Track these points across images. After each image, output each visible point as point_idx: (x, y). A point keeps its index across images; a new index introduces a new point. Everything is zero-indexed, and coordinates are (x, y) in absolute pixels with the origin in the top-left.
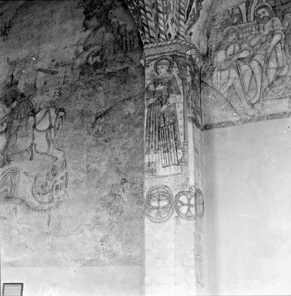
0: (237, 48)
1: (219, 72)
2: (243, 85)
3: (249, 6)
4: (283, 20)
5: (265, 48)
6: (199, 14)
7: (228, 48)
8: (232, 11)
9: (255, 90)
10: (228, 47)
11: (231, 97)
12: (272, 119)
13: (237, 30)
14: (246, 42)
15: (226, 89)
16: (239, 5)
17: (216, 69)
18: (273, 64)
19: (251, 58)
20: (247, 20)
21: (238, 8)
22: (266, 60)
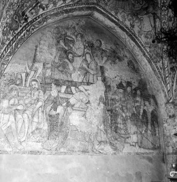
0: (17, 102)
1: (3, 114)
2: (17, 127)
3: (27, 76)
5: (33, 107)
9: (23, 133)
10: (11, 99)
11: (8, 134)
12: (31, 154)
13: (18, 89)
14: (22, 100)
15: (5, 128)
16: (21, 73)
18: (36, 119)
22: (32, 115)
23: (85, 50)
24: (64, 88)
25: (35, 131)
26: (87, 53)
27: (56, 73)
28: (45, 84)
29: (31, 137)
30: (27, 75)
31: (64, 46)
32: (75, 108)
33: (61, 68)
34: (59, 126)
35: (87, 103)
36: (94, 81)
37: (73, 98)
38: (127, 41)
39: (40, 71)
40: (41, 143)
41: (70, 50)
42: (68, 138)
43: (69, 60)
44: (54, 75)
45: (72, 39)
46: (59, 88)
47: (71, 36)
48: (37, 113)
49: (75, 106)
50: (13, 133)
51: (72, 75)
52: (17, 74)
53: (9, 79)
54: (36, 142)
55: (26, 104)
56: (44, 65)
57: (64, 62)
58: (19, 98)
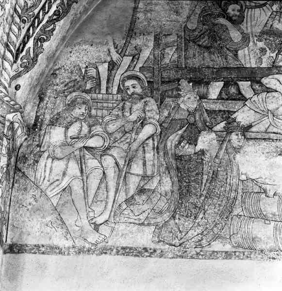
0: (85, 129)
1: (50, 160)
2: (85, 190)
3: (113, 69)
4: (161, 105)
5: (128, 141)
6: (37, 60)
7: (70, 125)
8: (86, 71)
10: (71, 124)
11: (63, 205)
12: (124, 254)
16: (98, 64)
17: (46, 155)
19: (106, 151)
20: (107, 90)
21: (97, 68)
24: (215, 89)
25: (137, 197)
27: (191, 52)
28: (163, 82)
29: (126, 212)
30: (113, 66)
32: (253, 135)
33: (205, 41)
34: (204, 181)
37: (246, 108)
39: (146, 54)
40: (153, 228)
42: (235, 212)
43: (230, 19)
44: (186, 58)
46: (203, 90)
48: (141, 152)
49: (253, 129)
50: (76, 203)
51: (239, 52)
52: (87, 67)
53: (67, 80)
54: (139, 224)
55: (110, 134)
56: (157, 39)
57: (214, 25)
58: (91, 121)
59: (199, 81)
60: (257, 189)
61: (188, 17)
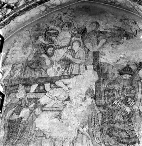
4: (8, 97)
23: (73, 39)
24: (34, 87)
26: (75, 41)
28: (11, 86)
31: (44, 42)
32: (46, 109)
34: (19, 132)
35: (66, 100)
36: (79, 71)
38: (137, 10)
41: (51, 43)
44: (24, 74)
45: (54, 31)
46: (28, 88)
47: (55, 28)
49: (47, 106)
51: (48, 70)
56: (13, 66)
59: (27, 84)
60: (42, 135)
61: (29, 55)
